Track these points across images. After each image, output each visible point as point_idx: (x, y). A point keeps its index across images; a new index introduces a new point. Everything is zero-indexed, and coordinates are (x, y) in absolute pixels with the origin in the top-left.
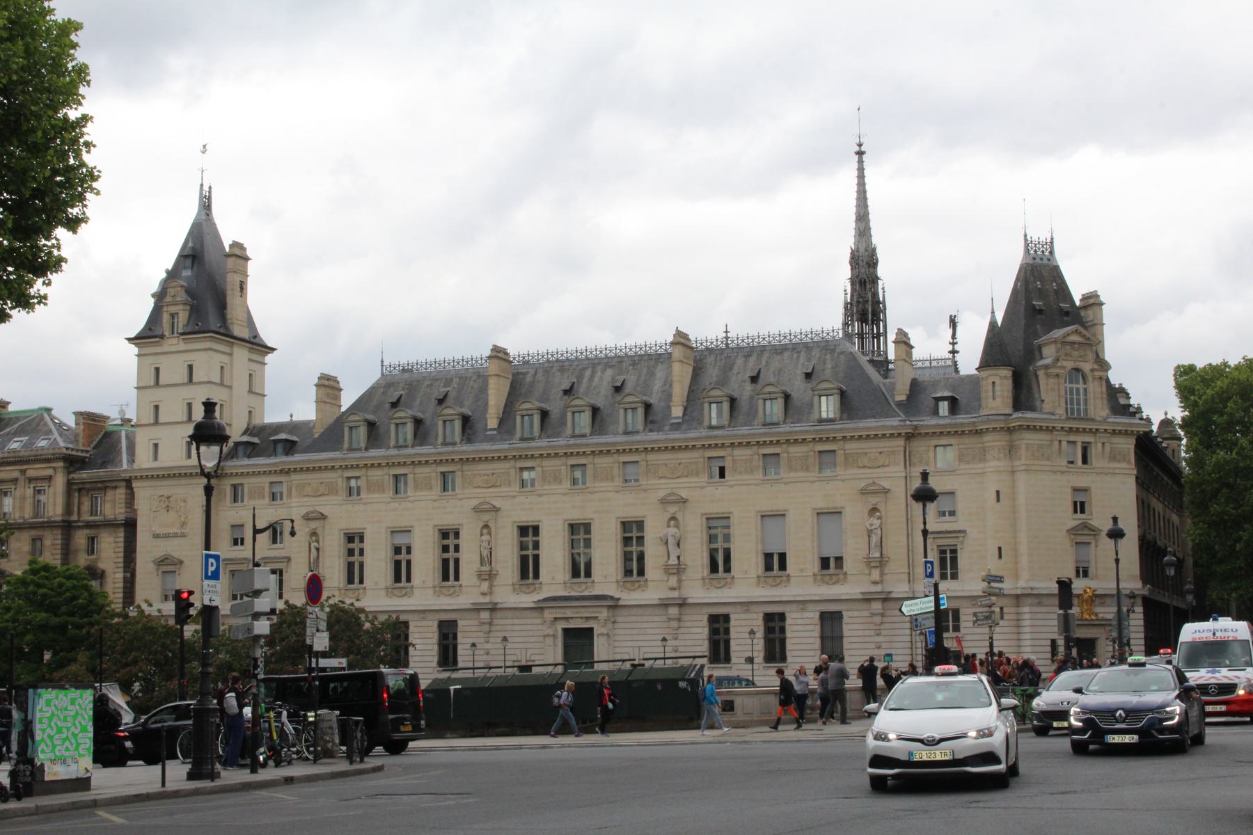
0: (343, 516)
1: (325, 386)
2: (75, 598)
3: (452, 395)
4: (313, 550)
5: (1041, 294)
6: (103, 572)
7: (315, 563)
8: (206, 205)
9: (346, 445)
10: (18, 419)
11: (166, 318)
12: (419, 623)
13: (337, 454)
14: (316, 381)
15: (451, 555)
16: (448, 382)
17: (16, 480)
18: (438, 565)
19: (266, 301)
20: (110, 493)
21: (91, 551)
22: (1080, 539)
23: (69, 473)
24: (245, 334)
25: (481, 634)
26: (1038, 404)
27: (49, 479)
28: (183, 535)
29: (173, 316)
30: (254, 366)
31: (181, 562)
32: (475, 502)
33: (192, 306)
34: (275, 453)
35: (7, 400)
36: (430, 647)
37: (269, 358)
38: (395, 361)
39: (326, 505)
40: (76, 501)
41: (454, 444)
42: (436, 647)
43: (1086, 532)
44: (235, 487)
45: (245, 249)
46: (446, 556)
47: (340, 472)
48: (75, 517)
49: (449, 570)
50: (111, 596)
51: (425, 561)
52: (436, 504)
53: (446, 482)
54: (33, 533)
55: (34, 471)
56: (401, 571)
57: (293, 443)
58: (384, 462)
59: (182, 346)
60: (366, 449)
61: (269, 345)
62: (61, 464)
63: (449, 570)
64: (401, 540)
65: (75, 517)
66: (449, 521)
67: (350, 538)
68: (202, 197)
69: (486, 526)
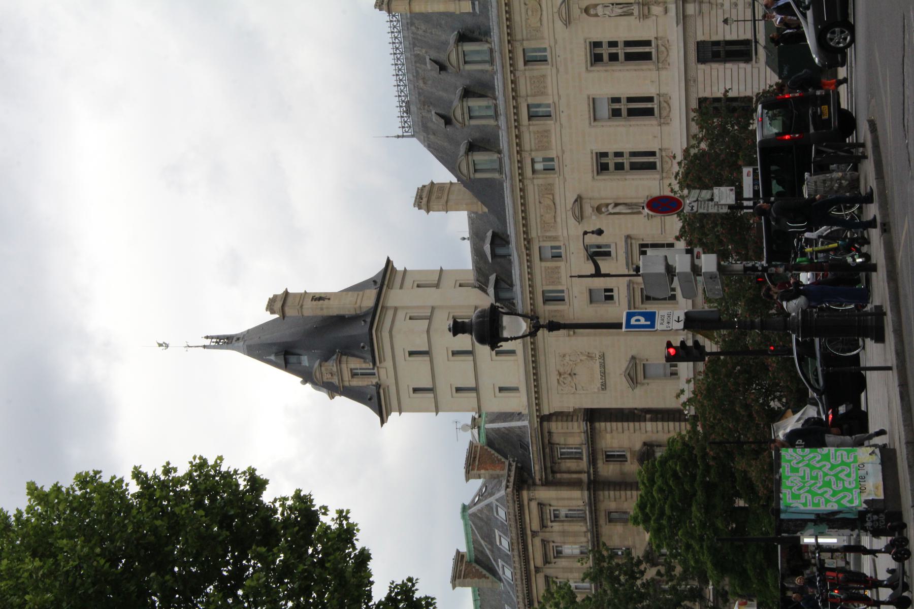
0: (577, 178)
1: (428, 201)
2: (675, 475)
3: (434, 54)
4: (617, 210)
6: (645, 444)
7: (633, 208)
8: (227, 341)
9: (496, 176)
10: (475, 541)
11: (356, 382)
12: (701, 86)
13: (507, 185)
14: (423, 212)
15: (620, 51)
16: (419, 59)
17: (543, 541)
18: (632, 65)
19: (332, 270)
20: (556, 439)
21: (621, 458)
23: (534, 484)
24: (372, 294)
25: (713, 12)
27: (541, 505)
28: (603, 356)
29: (354, 375)
30: (408, 282)
31: (633, 358)
32: (559, 24)
33: (343, 353)
34: (507, 257)
35: (454, 553)
36: (728, 72)
37: (399, 266)
38: (398, 123)
39: (565, 198)
40: (566, 476)
41: (491, 50)
42: (729, 65)
44: (546, 300)
45: (275, 297)
46: (621, 57)
47: (527, 182)
48: (584, 477)
49: (639, 53)
50: (673, 434)
51: (629, 81)
52: (562, 69)
53: (535, 59)
54: (602, 521)
55: (533, 521)
56: (640, 108)
57: (495, 236)
58: (514, 132)
59: (388, 363)
60: (499, 152)
61: (384, 266)
62: (525, 494)
63: (639, 53)
64: (604, 110)
65: (584, 477)
66: (581, 55)
67: (603, 168)
68: (218, 346)
69: (586, 10)
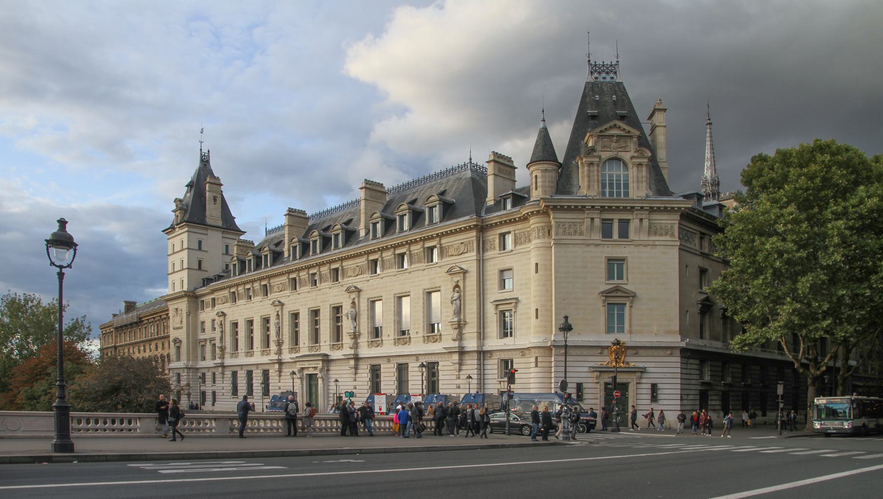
5: (598, 104)
22: (612, 300)
26: (575, 189)
43: (619, 294)
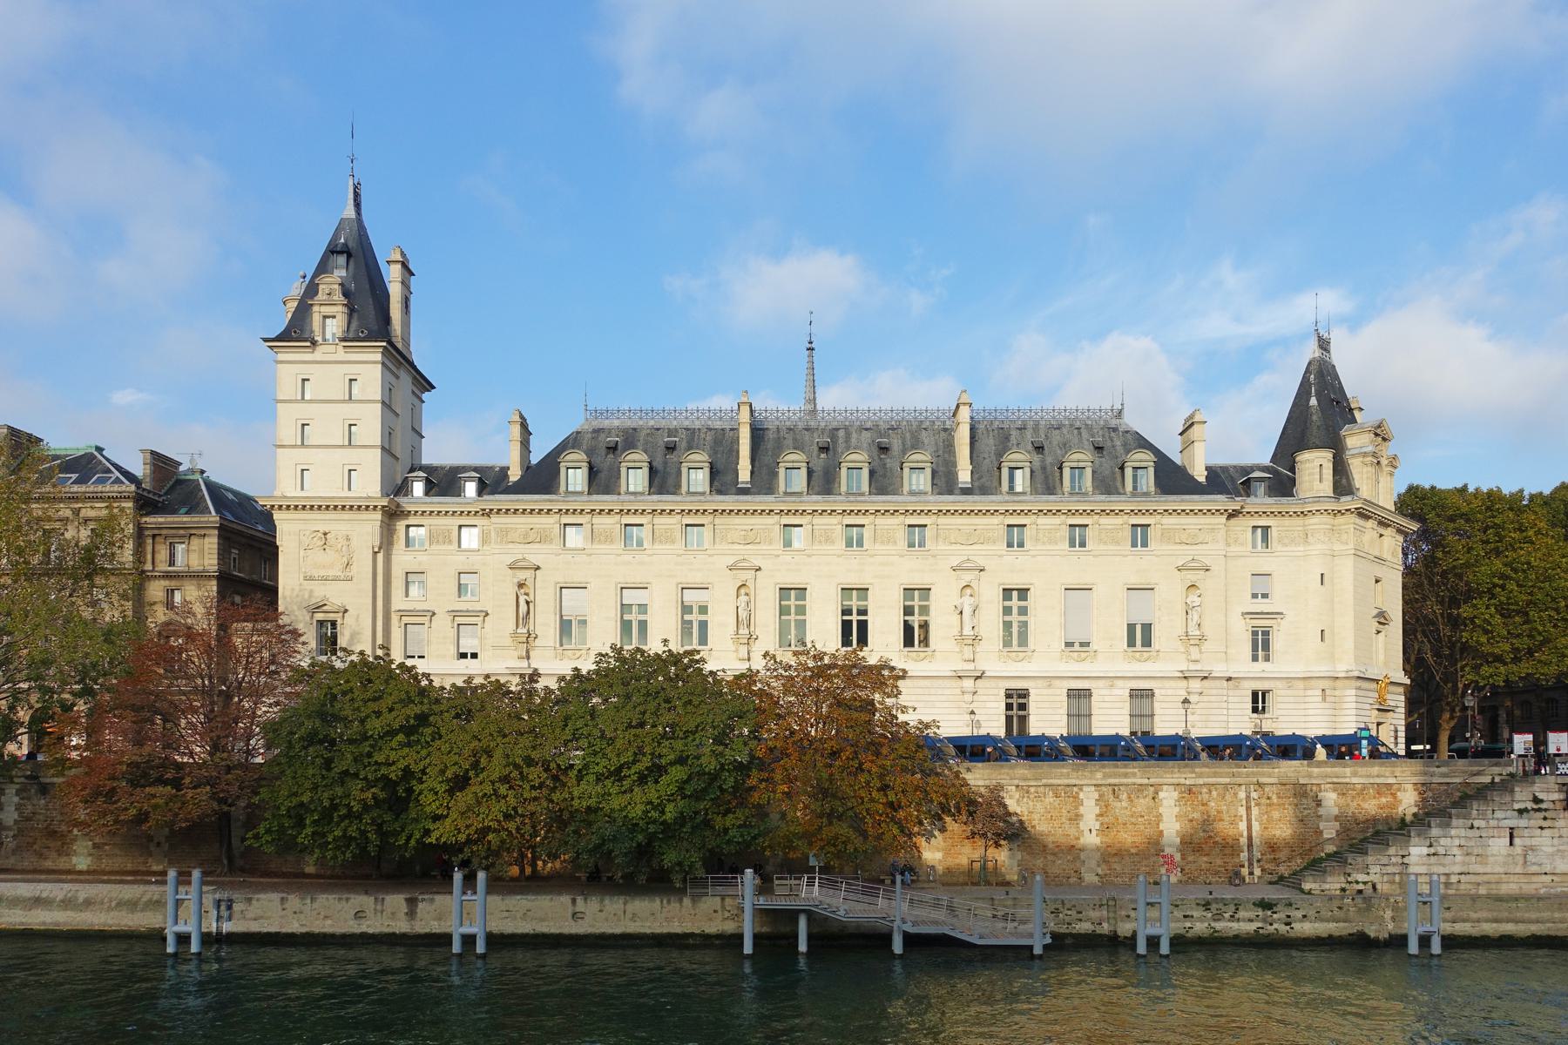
20: (195, 541)
40: (149, 548)
48: (148, 567)
